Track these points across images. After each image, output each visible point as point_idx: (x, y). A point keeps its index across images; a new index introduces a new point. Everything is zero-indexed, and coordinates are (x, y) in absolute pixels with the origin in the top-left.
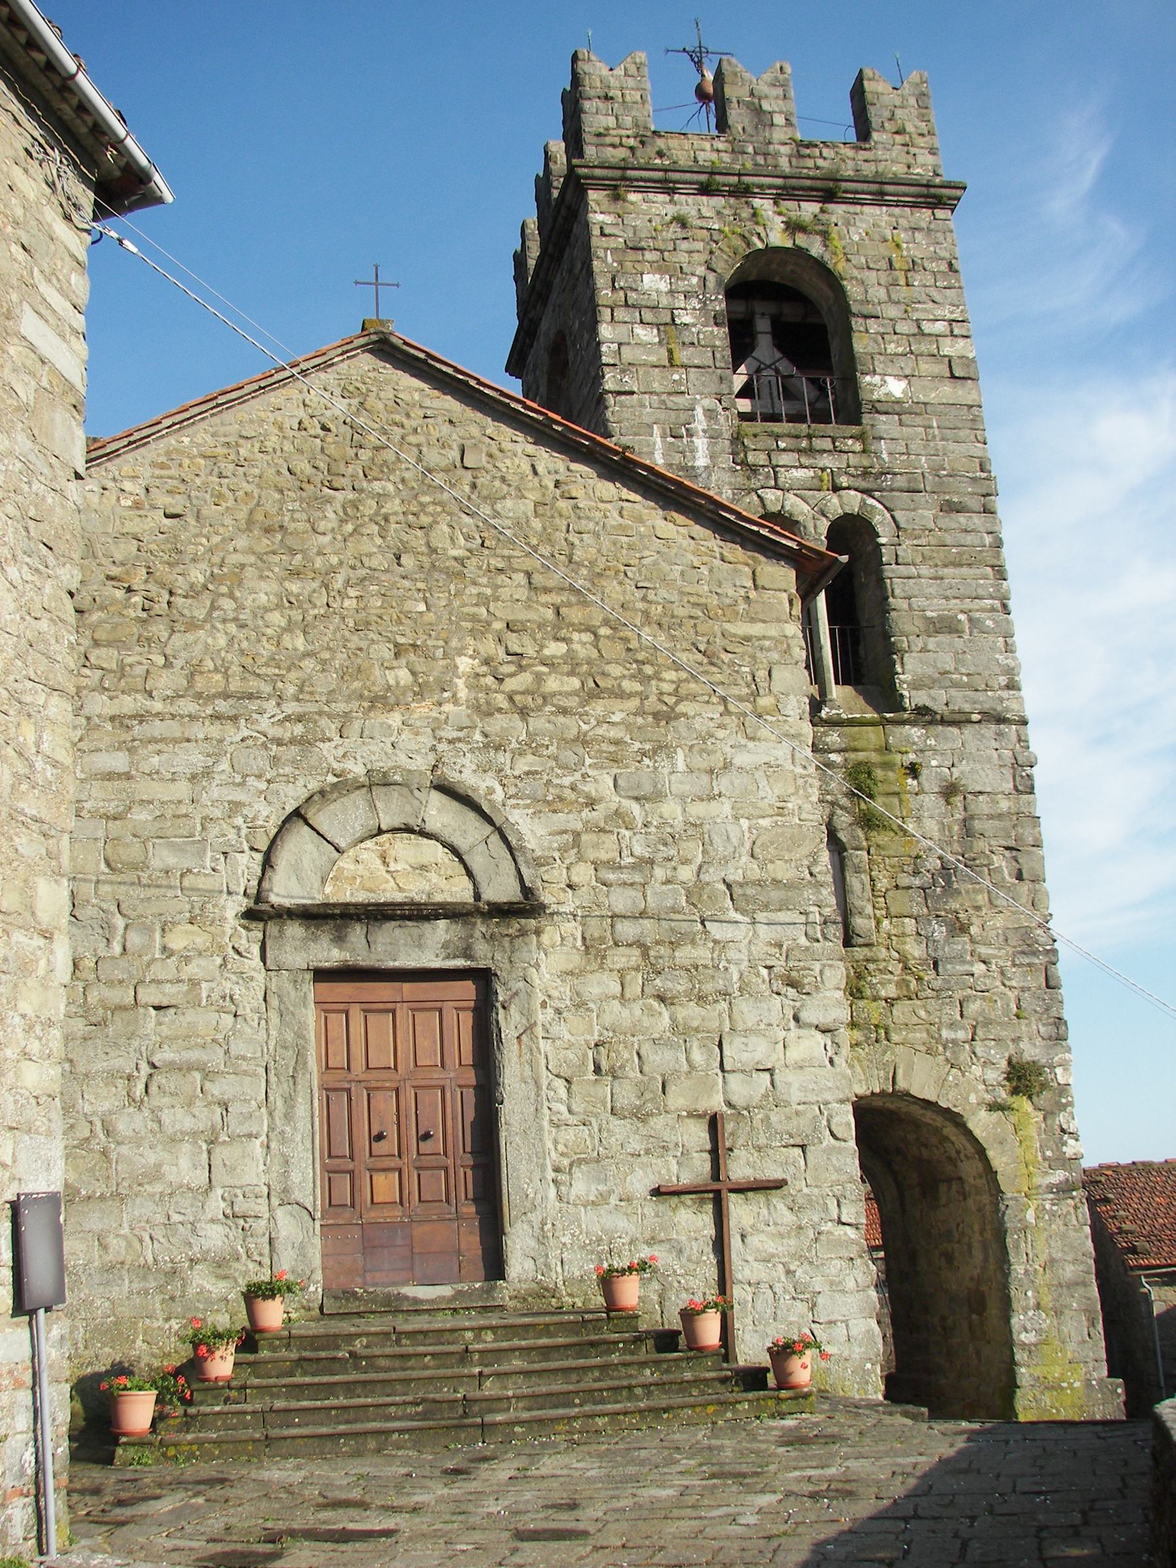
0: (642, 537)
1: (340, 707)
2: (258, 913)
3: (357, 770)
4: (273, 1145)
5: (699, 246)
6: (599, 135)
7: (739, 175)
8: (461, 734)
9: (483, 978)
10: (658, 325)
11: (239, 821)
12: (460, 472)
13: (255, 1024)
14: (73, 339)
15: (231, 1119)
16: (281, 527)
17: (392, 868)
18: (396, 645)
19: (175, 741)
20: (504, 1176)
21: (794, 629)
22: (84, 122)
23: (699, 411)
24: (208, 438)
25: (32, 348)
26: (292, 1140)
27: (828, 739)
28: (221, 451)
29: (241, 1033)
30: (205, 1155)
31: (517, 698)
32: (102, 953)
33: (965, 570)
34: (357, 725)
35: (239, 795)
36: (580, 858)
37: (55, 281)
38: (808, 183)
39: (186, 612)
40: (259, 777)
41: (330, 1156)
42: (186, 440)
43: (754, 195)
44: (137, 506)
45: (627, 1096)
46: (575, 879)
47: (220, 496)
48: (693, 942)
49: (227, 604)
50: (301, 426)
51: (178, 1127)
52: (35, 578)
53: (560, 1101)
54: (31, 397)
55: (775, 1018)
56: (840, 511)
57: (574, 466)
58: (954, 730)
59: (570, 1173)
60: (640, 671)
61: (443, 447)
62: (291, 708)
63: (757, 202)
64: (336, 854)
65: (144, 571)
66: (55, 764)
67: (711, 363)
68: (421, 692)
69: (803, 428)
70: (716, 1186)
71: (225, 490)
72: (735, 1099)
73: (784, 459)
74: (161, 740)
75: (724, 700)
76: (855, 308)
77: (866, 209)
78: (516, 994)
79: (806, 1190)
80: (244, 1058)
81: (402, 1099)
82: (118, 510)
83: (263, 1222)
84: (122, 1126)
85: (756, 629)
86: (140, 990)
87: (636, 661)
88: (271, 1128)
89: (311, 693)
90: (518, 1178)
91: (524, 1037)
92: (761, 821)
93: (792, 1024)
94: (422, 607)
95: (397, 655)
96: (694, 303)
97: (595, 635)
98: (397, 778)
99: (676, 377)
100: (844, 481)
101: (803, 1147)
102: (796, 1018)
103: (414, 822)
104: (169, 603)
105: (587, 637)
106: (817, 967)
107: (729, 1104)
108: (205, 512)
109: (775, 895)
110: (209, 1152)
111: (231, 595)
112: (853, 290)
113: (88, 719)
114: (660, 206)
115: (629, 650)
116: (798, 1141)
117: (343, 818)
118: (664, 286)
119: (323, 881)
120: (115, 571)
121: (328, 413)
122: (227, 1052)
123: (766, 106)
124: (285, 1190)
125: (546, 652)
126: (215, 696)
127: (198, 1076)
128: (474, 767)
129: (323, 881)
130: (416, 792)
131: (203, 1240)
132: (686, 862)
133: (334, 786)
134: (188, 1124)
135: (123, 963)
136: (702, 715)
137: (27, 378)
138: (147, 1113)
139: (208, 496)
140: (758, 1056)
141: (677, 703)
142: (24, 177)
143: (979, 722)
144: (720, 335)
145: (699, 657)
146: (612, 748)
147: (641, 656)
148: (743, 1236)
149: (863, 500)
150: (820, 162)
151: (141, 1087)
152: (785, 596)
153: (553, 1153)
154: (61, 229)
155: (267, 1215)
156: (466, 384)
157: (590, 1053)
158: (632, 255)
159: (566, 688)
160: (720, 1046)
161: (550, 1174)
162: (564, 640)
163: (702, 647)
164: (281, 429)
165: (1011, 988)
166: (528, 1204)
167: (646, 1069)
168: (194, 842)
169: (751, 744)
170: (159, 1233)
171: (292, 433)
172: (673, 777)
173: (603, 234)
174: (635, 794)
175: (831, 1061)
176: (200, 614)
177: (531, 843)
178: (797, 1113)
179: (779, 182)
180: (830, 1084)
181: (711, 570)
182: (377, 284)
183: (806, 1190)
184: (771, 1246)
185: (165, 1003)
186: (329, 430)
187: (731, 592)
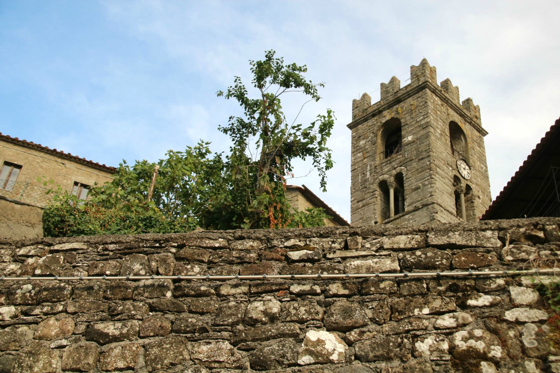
33: (422, 173)
63: (384, 112)
143: (422, 208)
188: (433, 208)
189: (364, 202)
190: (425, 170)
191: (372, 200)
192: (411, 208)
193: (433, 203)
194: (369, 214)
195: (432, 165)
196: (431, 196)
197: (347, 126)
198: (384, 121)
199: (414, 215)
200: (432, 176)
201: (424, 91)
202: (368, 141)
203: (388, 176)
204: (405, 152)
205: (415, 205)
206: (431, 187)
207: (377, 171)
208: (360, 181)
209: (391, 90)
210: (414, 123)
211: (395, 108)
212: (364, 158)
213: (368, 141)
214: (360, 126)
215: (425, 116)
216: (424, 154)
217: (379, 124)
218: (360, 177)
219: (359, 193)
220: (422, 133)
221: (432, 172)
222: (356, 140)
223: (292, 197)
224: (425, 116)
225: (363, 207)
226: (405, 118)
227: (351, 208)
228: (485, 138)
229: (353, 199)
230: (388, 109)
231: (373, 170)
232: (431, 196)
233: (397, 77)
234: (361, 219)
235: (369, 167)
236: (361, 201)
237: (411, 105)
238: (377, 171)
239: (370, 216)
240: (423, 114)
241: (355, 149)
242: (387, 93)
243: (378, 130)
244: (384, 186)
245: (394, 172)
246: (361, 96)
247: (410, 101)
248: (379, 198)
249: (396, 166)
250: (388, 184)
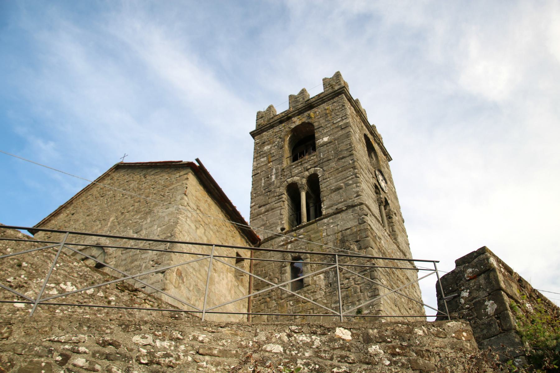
33: (344, 172)
58: (339, 215)
63: (293, 119)
114: (271, 131)
143: (346, 209)
165: (358, 284)
188: (362, 209)
189: (268, 206)
190: (348, 169)
191: (278, 204)
192: (330, 211)
193: (361, 204)
194: (273, 220)
195: (356, 163)
196: (357, 197)
197: (250, 133)
198: (293, 126)
199: (335, 218)
200: (358, 175)
201: (340, 96)
202: (274, 146)
203: (298, 178)
204: (320, 153)
205: (336, 207)
206: (357, 186)
207: (285, 174)
208: (263, 185)
209: (301, 100)
210: (329, 125)
211: (306, 114)
212: (269, 162)
213: (274, 146)
215: (343, 118)
216: (345, 153)
217: (287, 129)
218: (263, 181)
219: (261, 197)
220: (340, 133)
221: (356, 170)
222: (260, 147)
223: (180, 176)
224: (343, 118)
225: (265, 212)
226: (319, 122)
227: (251, 214)
228: (390, 163)
229: (253, 204)
230: (298, 115)
231: (280, 173)
232: (357, 197)
233: (307, 90)
234: (263, 225)
235: (274, 170)
236: (264, 205)
237: (325, 109)
238: (285, 174)
239: (275, 221)
240: (341, 116)
241: (258, 154)
243: (285, 135)
244: (293, 191)
245: (307, 174)
246: (267, 107)
247: (324, 106)
248: (286, 203)
249: (309, 167)
250: (299, 186)
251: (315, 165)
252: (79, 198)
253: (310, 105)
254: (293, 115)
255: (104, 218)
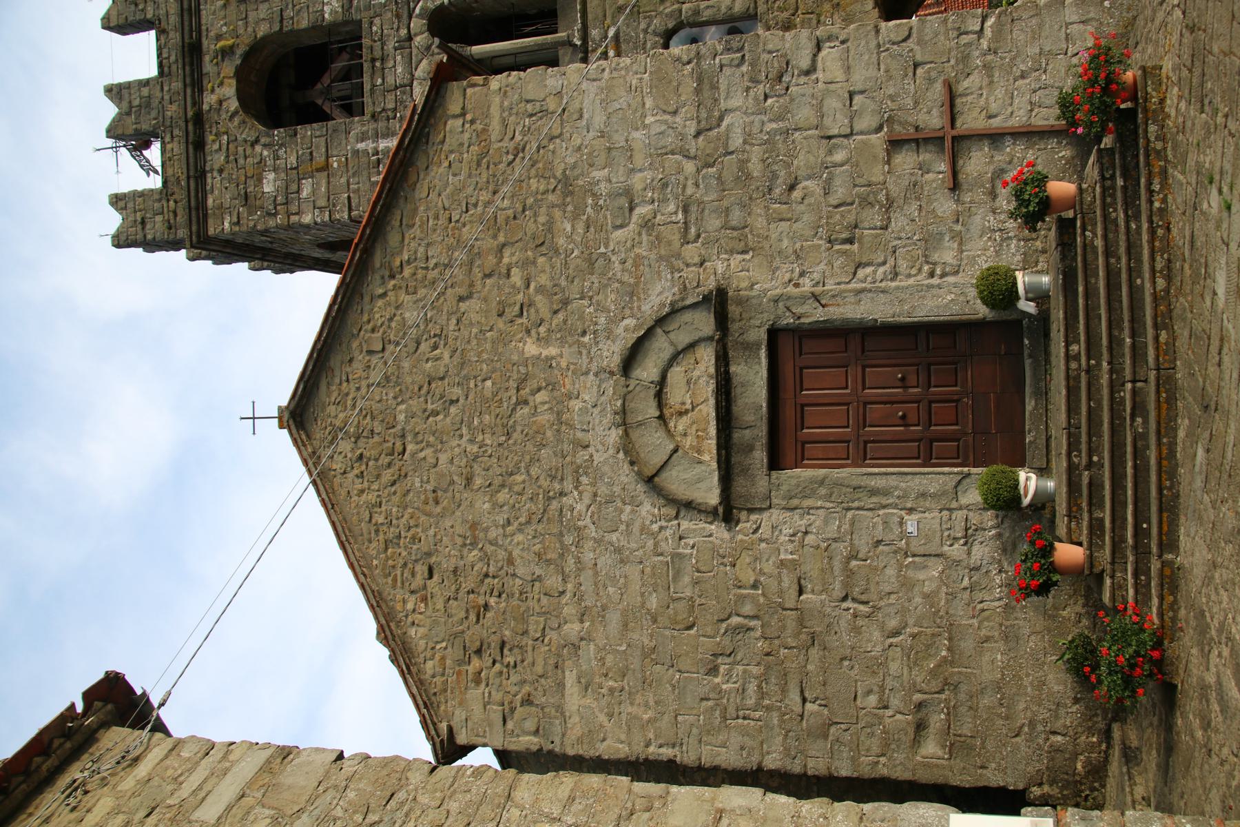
0: (428, 209)
1: (566, 447)
2: (727, 513)
3: (615, 435)
4: (909, 505)
5: (240, 149)
6: (170, 228)
7: (187, 121)
8: (584, 352)
9: (774, 334)
10: (299, 180)
11: (655, 527)
12: (387, 354)
13: (813, 518)
14: (231, 757)
15: (887, 538)
16: (434, 491)
17: (688, 406)
18: (518, 403)
19: (596, 574)
20: (937, 319)
21: (496, 82)
22: (61, 745)
23: (361, 146)
24: (374, 544)
25: (229, 808)
26: (905, 491)
27: (597, 38)
28: (381, 537)
29: (819, 528)
30: (917, 559)
31: (555, 307)
32: (759, 633)
34: (579, 435)
35: (636, 528)
36: (678, 256)
37: (182, 779)
38: (187, 68)
39: (500, 565)
40: (622, 511)
41: (918, 458)
42: (375, 562)
43: (201, 109)
44: (424, 599)
45: (873, 217)
46: (697, 260)
47: (413, 538)
48: (748, 161)
49: (493, 534)
50: (361, 475)
51: (893, 580)
52: (413, 816)
53: (875, 272)
54: (267, 812)
55: (808, 90)
56: (426, 34)
57: (378, 265)
59: (935, 264)
60: (531, 208)
61: (369, 367)
62: (568, 485)
63: (205, 107)
64: (680, 452)
65: (471, 596)
66: (572, 799)
67: (323, 139)
68: (552, 386)
69: (366, 66)
70: (948, 143)
71: (409, 535)
72: (874, 125)
73: (390, 80)
74: (596, 584)
75: (552, 138)
76: (276, 28)
77: (204, 21)
78: (788, 309)
79: (953, 62)
80: (839, 527)
81: (873, 399)
82: (428, 613)
83: (971, 514)
84: (893, 623)
85: (495, 111)
86: (787, 606)
87: (524, 211)
88: (896, 506)
89: (557, 470)
90: (938, 307)
91: (823, 302)
92: (647, 106)
93: (814, 77)
94: (489, 383)
95: (526, 402)
96: (281, 152)
97: (504, 245)
98: (619, 403)
99: (335, 165)
100: (403, 32)
101: (916, 66)
102: (807, 73)
103: (652, 392)
104: (494, 577)
105: (507, 252)
106: (765, 56)
107: (879, 129)
108: (425, 549)
109: (706, 93)
110: (914, 556)
111: (486, 530)
112: (263, 30)
113: (582, 639)
115: (515, 218)
116: (911, 70)
117: (654, 445)
118: (272, 176)
119: (700, 462)
120: (473, 617)
121: (349, 455)
122: (835, 540)
123: (136, 102)
124: (944, 493)
125: (519, 284)
126: (561, 542)
127: (854, 563)
128: (609, 342)
129: (700, 462)
130: (630, 388)
131: (985, 562)
132: (680, 171)
133: (626, 453)
134: (891, 571)
135: (766, 618)
136: (563, 156)
137: (251, 818)
138: (882, 603)
139: (415, 547)
140: (839, 105)
141: (555, 177)
142: (95, 810)
144: (307, 132)
145: (518, 160)
146: (592, 229)
147: (519, 207)
148: (990, 117)
149: (417, 16)
150: (173, 58)
151: (862, 608)
152: (469, 91)
153: (919, 278)
154: (143, 770)
155: (965, 512)
156: (321, 350)
157: (837, 247)
158: (251, 200)
159: (548, 269)
160: (830, 138)
161: (936, 281)
162: (509, 270)
163: (511, 157)
164: (362, 491)
166: (962, 298)
167: (849, 200)
168: (673, 562)
169: (586, 116)
170: (979, 596)
171: (366, 483)
172: (614, 180)
173: (238, 223)
174: (627, 211)
175: (843, 42)
176: (502, 554)
177: (668, 297)
178: (887, 71)
179: (189, 91)
180: (863, 42)
181: (452, 152)
182: (254, 418)
183: (953, 62)
184: (1000, 92)
185: (796, 587)
186: (361, 455)
187: (467, 135)
198: (234, 104)
202: (277, 158)
211: (208, 66)
214: (210, 202)
230: (201, 91)
242: (148, 105)
251: (405, 15)
252: (370, 567)
253: (186, 57)
254: (194, 104)
255: (513, 384)
